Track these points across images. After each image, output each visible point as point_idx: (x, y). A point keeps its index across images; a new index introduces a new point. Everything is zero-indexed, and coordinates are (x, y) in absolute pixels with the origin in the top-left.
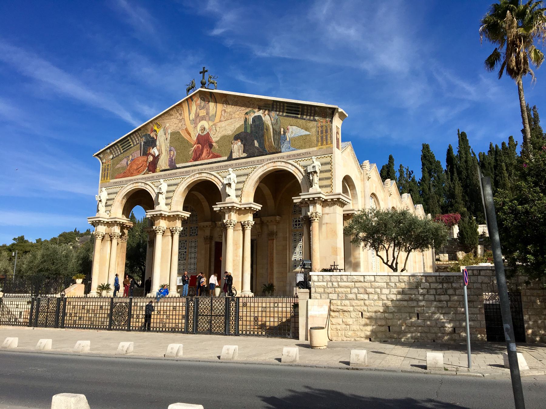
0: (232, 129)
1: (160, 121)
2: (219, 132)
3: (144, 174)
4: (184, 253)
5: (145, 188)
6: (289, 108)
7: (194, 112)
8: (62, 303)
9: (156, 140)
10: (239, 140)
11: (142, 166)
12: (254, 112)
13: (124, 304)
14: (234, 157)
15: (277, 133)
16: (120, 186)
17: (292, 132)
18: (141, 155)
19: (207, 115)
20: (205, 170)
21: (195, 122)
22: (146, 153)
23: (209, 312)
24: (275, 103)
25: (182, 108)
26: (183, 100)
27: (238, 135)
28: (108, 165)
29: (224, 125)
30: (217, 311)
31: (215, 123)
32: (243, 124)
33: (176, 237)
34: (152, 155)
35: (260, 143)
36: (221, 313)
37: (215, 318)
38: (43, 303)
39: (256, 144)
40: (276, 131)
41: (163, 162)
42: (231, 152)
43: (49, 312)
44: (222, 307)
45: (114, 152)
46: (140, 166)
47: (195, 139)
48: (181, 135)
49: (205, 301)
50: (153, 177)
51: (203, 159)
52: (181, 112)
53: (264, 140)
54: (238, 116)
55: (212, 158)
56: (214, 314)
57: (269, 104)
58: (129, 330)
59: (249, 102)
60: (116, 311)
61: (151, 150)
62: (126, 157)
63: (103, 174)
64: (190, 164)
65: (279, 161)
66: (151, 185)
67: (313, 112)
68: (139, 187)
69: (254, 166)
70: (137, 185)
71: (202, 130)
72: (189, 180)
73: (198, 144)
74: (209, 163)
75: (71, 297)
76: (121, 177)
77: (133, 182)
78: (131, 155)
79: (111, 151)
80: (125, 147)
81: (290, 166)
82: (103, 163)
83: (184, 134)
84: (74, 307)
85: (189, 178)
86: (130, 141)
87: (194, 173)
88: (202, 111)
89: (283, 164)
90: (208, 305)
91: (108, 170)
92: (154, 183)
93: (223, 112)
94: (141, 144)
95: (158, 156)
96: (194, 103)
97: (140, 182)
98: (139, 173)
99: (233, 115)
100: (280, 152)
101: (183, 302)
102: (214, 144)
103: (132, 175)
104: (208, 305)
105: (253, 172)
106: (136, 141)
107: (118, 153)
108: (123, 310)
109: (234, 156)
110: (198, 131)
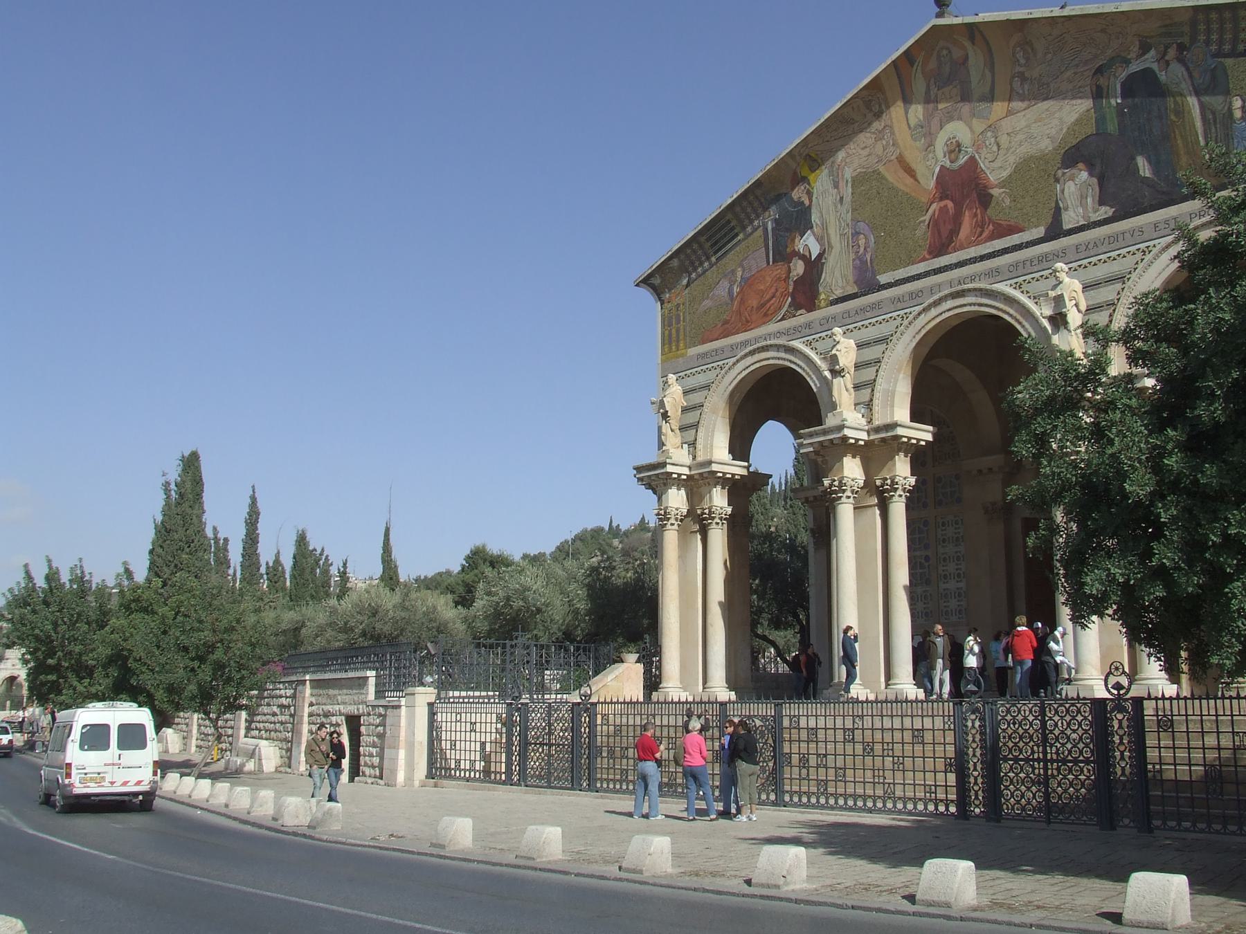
0: (1054, 131)
2: (1008, 149)
4: (923, 561)
8: (585, 718)
9: (810, 207)
10: (1081, 165)
11: (773, 297)
12: (1127, 62)
13: (758, 723)
14: (1067, 226)
20: (972, 280)
21: (926, 133)
22: (783, 254)
23: (1035, 748)
24: (1201, 17)
26: (883, 66)
27: (1076, 147)
28: (678, 305)
29: (1023, 123)
30: (1063, 745)
31: (990, 123)
32: (1088, 111)
33: (898, 509)
34: (803, 257)
36: (1081, 752)
37: (1058, 769)
38: (536, 718)
39: (1144, 168)
40: (1214, 113)
41: (837, 274)
42: (1057, 212)
43: (553, 745)
44: (1080, 732)
46: (768, 297)
47: (932, 184)
48: (886, 180)
49: (1019, 712)
50: (808, 325)
51: (962, 248)
52: (880, 106)
55: (992, 237)
56: (1055, 757)
58: (779, 803)
59: (1103, 31)
61: (797, 240)
62: (725, 276)
63: (667, 332)
64: (921, 268)
68: (771, 362)
69: (1142, 246)
71: (951, 152)
72: (923, 319)
73: (941, 199)
75: (608, 700)
77: (751, 348)
78: (741, 265)
80: (720, 244)
83: (895, 177)
87: (936, 297)
88: (946, 90)
90: (1031, 725)
91: (678, 322)
93: (1017, 83)
94: (766, 229)
95: (820, 256)
98: (766, 317)
99: (1052, 85)
101: (943, 716)
102: (995, 192)
103: (746, 326)
104: (1031, 725)
105: (1140, 266)
109: (1070, 219)
110: (941, 157)
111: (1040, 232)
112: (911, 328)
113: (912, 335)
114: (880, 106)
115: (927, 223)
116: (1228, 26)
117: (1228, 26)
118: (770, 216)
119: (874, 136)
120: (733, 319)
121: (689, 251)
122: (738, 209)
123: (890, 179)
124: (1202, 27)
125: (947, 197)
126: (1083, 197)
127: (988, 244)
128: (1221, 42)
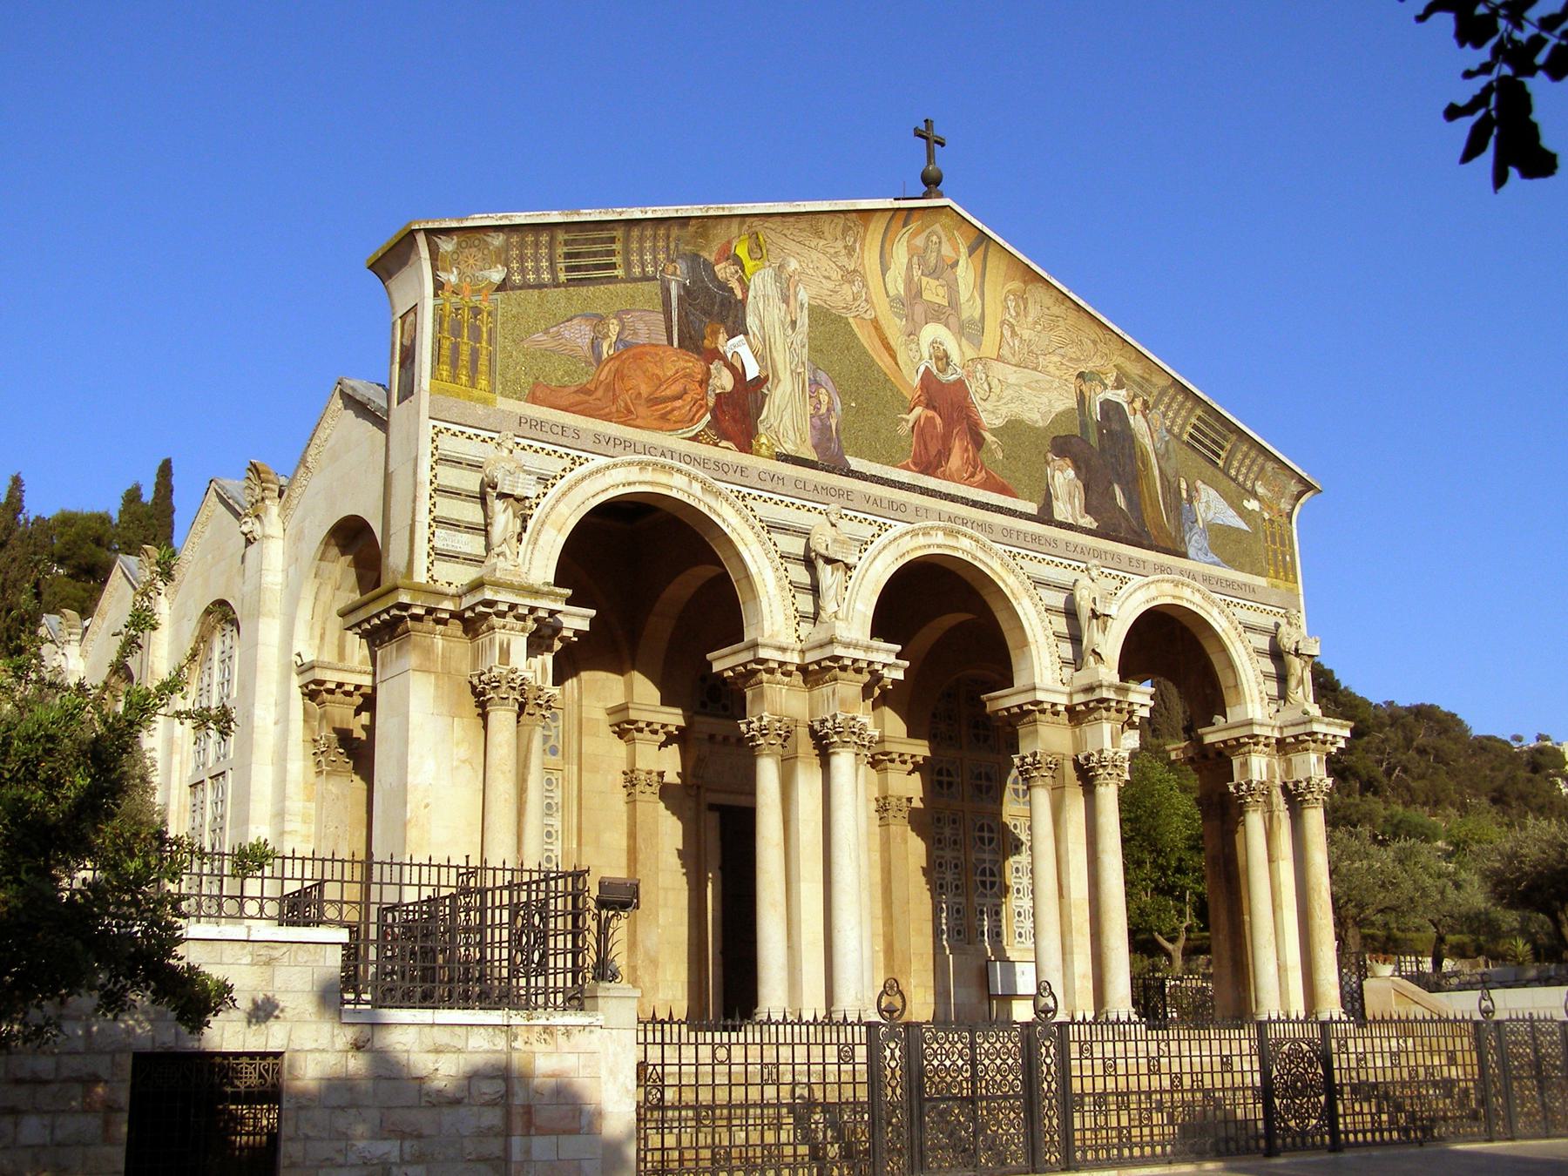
0: (1043, 409)
1: (772, 235)
3: (694, 439)
5: (706, 510)
6: (1202, 426)
7: (903, 274)
9: (743, 303)
15: (1171, 490)
16: (562, 450)
17: (1208, 507)
18: (671, 342)
19: (949, 311)
25: (861, 230)
34: (731, 367)
35: (1129, 501)
45: (522, 259)
46: (668, 393)
47: (917, 381)
51: (950, 478)
52: (855, 241)
53: (1140, 494)
54: (1057, 373)
57: (1154, 385)
59: (1094, 342)
60: (1282, 1078)
61: (722, 337)
62: (586, 317)
63: (446, 344)
65: (1188, 586)
66: (740, 503)
67: (1255, 468)
68: (674, 494)
70: (663, 478)
73: (927, 406)
74: (975, 504)
76: (565, 403)
77: (644, 458)
79: (507, 247)
81: (1215, 612)
82: (439, 286)
84: (1109, 1068)
85: (908, 537)
86: (617, 247)
89: (1197, 598)
92: (749, 501)
93: (1007, 333)
94: (666, 291)
95: (760, 382)
96: (906, 235)
97: (679, 471)
98: (665, 422)
100: (1184, 555)
102: (988, 436)
103: (626, 418)
106: (643, 266)
107: (537, 271)
108: (1305, 1069)
109: (1061, 511)
111: (1031, 508)
112: (892, 546)
113: (896, 556)
114: (855, 241)
115: (911, 424)
116: (1183, 413)
117: (1183, 413)
118: (674, 274)
119: (841, 273)
120: (600, 393)
121: (530, 238)
122: (635, 233)
123: (863, 340)
124: (1166, 400)
125: (934, 409)
126: (1071, 497)
127: (981, 492)
128: (1173, 422)
